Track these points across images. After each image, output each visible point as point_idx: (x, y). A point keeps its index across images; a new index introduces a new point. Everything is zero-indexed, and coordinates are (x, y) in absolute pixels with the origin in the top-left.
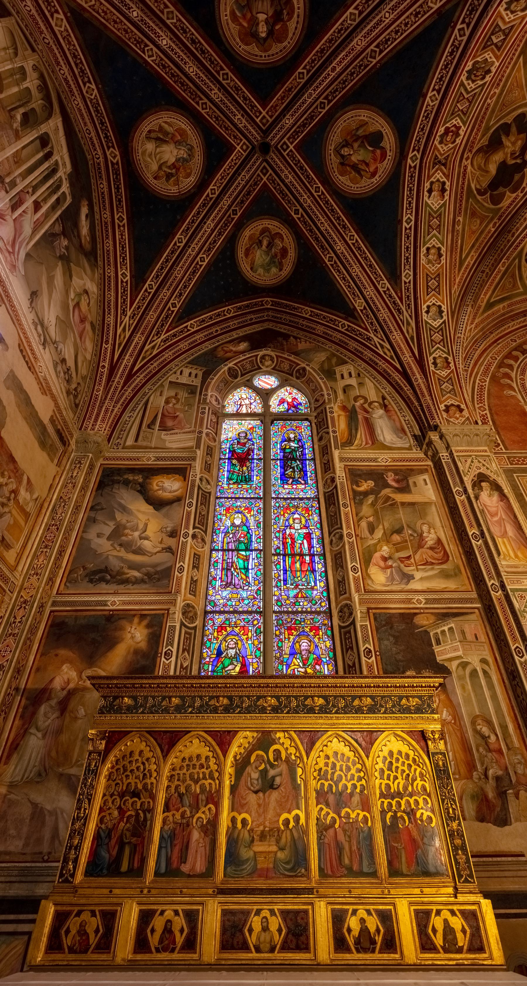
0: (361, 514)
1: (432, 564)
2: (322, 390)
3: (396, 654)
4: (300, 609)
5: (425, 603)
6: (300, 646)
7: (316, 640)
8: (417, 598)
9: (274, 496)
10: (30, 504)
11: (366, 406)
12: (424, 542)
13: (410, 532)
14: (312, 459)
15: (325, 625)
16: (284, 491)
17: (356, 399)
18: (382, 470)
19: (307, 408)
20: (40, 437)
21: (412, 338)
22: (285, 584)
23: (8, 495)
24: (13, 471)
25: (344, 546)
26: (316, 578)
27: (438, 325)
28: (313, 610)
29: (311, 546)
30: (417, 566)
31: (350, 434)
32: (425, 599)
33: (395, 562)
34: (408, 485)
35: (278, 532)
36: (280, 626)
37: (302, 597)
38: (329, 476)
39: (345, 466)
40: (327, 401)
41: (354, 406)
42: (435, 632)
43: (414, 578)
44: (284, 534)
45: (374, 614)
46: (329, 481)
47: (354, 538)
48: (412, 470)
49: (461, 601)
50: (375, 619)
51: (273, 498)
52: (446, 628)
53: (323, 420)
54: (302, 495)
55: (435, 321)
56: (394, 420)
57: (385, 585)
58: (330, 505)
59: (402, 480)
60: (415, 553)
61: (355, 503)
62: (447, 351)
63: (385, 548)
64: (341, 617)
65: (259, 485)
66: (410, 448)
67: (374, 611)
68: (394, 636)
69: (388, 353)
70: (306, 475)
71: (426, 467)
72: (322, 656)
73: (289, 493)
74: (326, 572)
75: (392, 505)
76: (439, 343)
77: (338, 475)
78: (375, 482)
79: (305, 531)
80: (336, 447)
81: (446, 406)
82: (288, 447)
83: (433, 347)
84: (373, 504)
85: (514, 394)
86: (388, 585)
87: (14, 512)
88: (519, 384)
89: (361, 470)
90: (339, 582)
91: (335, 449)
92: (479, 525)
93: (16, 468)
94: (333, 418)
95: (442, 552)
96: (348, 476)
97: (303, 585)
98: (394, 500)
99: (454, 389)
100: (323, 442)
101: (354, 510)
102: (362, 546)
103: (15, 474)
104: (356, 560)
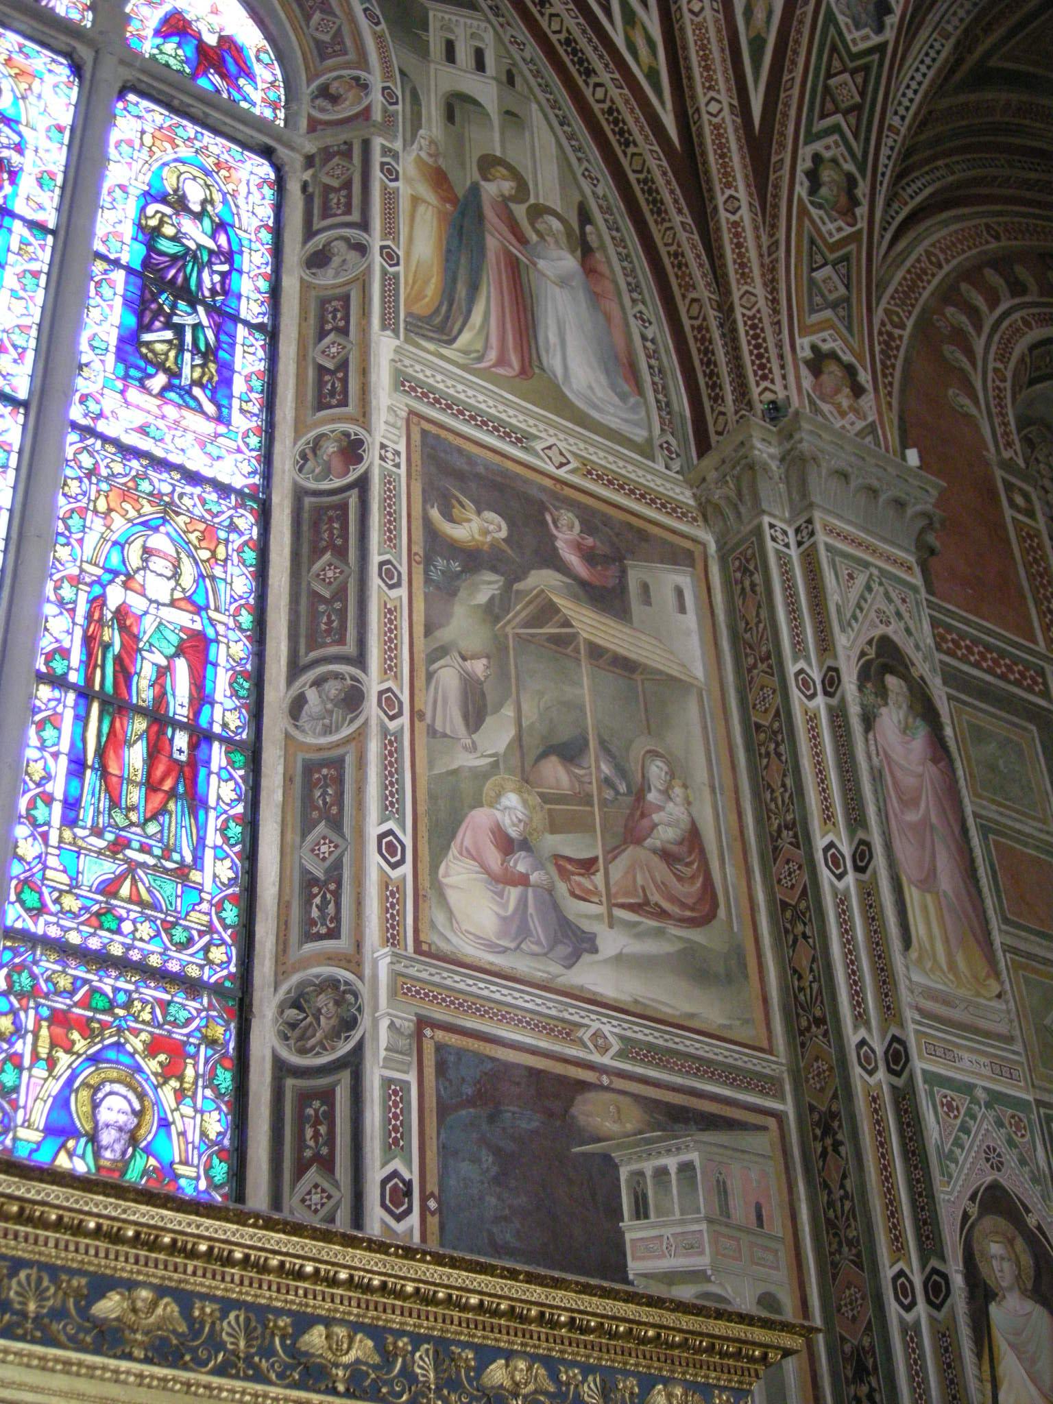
0: (445, 635)
1: (662, 914)
2: (362, 61)
3: (497, 1220)
4: (117, 950)
5: (621, 1055)
6: (95, 1106)
7: (167, 1095)
8: (596, 1025)
9: (76, 413)
11: (520, 211)
12: (645, 823)
13: (606, 769)
14: (260, 327)
15: (212, 1043)
16: (123, 413)
17: (488, 164)
18: (543, 489)
19: (274, 106)
21: (757, 45)
22: (70, 821)
25: (360, 737)
26: (201, 840)
27: (863, 46)
28: (174, 967)
29: (201, 697)
30: (611, 906)
31: (448, 293)
32: (622, 1038)
33: (539, 865)
34: (622, 588)
35: (76, 581)
36: (21, 996)
37: (135, 899)
38: (332, 425)
39: (412, 412)
40: (377, 115)
41: (475, 190)
42: (635, 1167)
43: (595, 950)
44: (98, 602)
45: (439, 1048)
46: (330, 448)
47: (405, 720)
48: (643, 536)
49: (732, 1075)
50: (441, 1068)
51: (74, 426)
52: (672, 1163)
53: (348, 185)
54: (196, 462)
55: (858, 28)
56: (608, 318)
57: (491, 947)
58: (317, 552)
59: (606, 560)
60: (613, 853)
61: (428, 580)
62: (859, 155)
63: (511, 800)
64: (293, 1026)
65: (19, 340)
66: (646, 450)
67: (440, 1035)
68: (497, 1152)
69: (643, 51)
70: (227, 382)
71: (688, 544)
72: (181, 1169)
73: (143, 430)
74: (251, 822)
75: (557, 640)
76: (846, 113)
77: (378, 439)
78: (512, 525)
79: (184, 618)
80: (388, 323)
81: (814, 348)
82: (169, 230)
83: (823, 116)
84: (493, 612)
85: (973, 411)
86: (505, 950)
88: (990, 384)
89: (470, 460)
90: (309, 882)
91: (384, 327)
92: (856, 820)
94: (390, 198)
95: (699, 883)
96: (416, 457)
97: (145, 850)
98: (567, 624)
99: (847, 300)
100: (327, 279)
101: (419, 605)
102: (431, 764)
104: (401, 812)
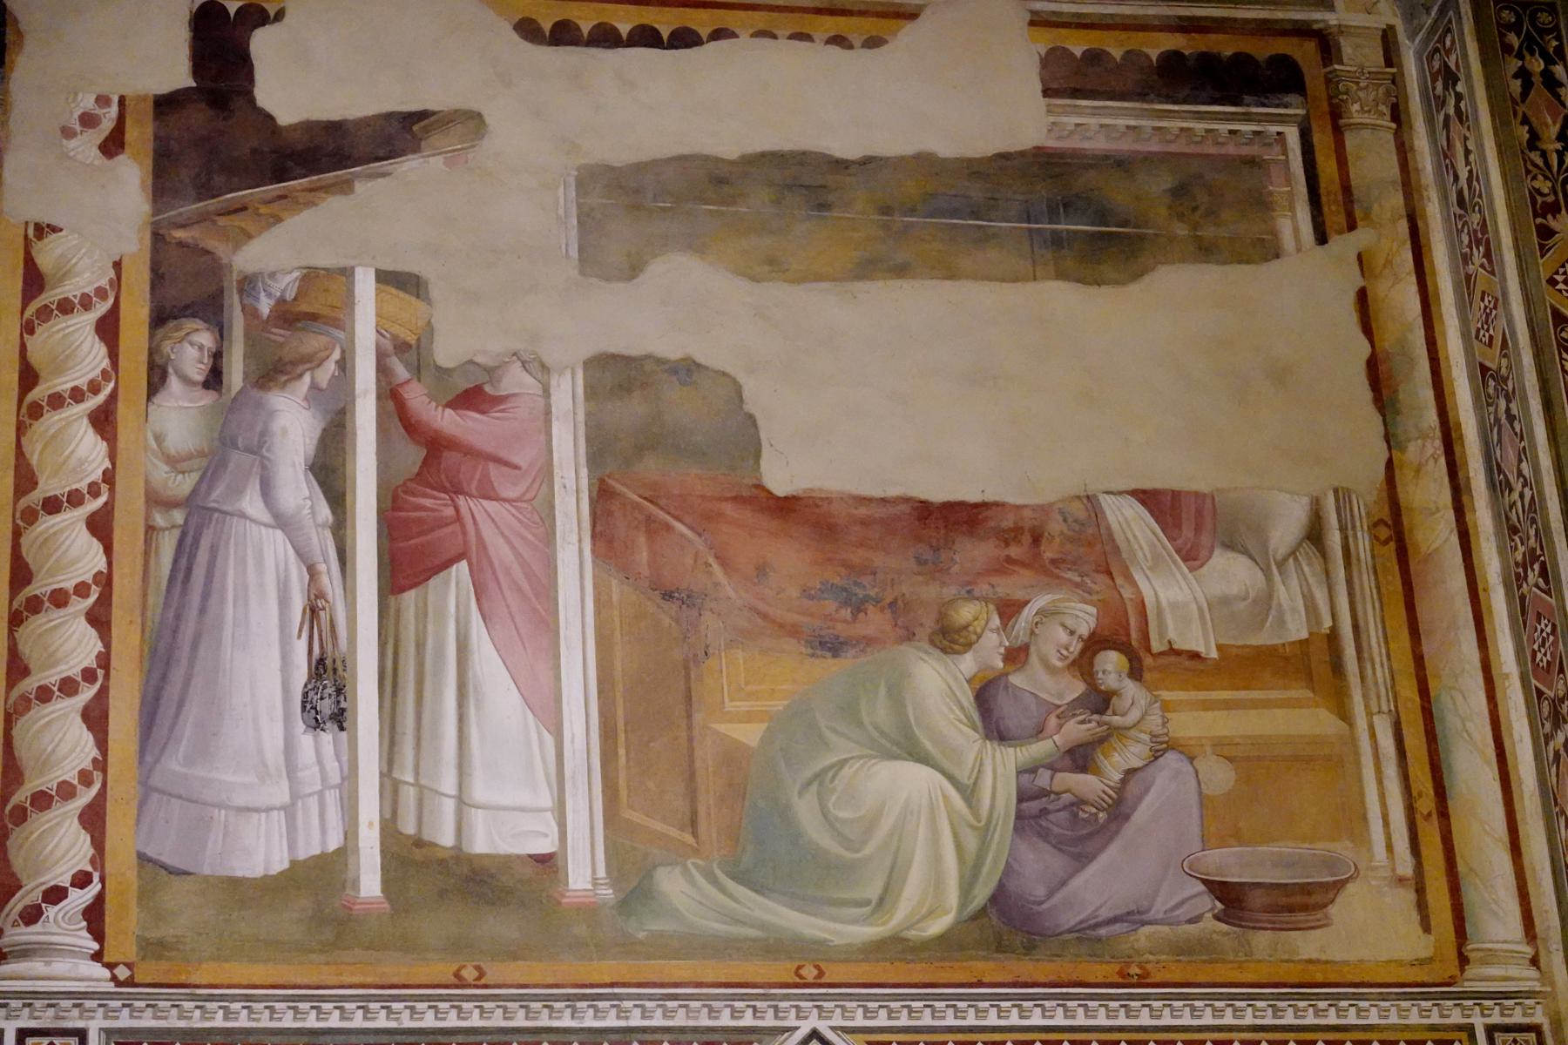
10: (1288, 595)
20: (1057, 241)
23: (1077, 688)
24: (1006, 566)
87: (1189, 725)
93: (1009, 536)
103: (1033, 563)
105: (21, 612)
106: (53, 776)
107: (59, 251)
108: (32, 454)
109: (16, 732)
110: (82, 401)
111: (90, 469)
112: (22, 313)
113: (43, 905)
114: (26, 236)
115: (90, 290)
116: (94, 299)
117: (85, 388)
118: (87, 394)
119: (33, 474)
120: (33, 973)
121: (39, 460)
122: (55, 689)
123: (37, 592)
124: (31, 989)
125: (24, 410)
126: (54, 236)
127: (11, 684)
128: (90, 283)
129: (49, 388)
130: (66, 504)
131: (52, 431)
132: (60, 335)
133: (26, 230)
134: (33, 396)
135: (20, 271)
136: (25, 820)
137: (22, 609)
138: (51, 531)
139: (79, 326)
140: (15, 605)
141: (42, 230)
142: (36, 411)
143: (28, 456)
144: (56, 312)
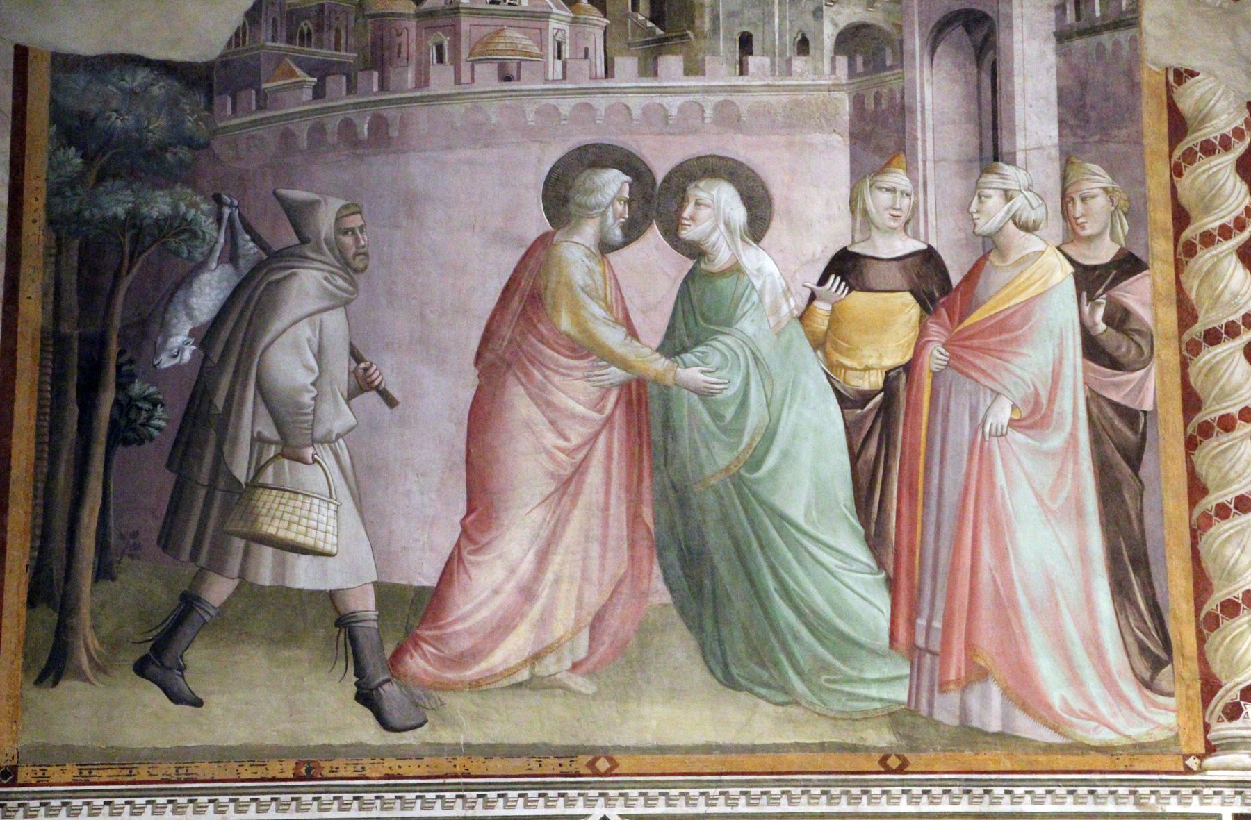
105: (1195, 437)
106: (1237, 586)
107: (1198, 94)
108: (1190, 291)
109: (1202, 547)
110: (1231, 237)
111: (1242, 301)
112: (1170, 157)
113: (1242, 703)
114: (1167, 83)
115: (1228, 130)
116: (1233, 139)
117: (1232, 225)
118: (1234, 231)
119: (1193, 309)
120: (1240, 764)
121: (1197, 295)
122: (1232, 506)
123: (1207, 418)
124: (1241, 779)
125: (1180, 248)
126: (1193, 80)
127: (1193, 503)
128: (1227, 125)
129: (1200, 228)
130: (1224, 336)
131: (1205, 268)
132: (1206, 175)
133: (1167, 77)
134: (1187, 234)
135: (1165, 116)
136: (1218, 626)
137: (1195, 434)
138: (1214, 361)
139: (1219, 167)
140: (1190, 430)
141: (1182, 75)
142: (1190, 249)
143: (1187, 292)
144: (1199, 154)
